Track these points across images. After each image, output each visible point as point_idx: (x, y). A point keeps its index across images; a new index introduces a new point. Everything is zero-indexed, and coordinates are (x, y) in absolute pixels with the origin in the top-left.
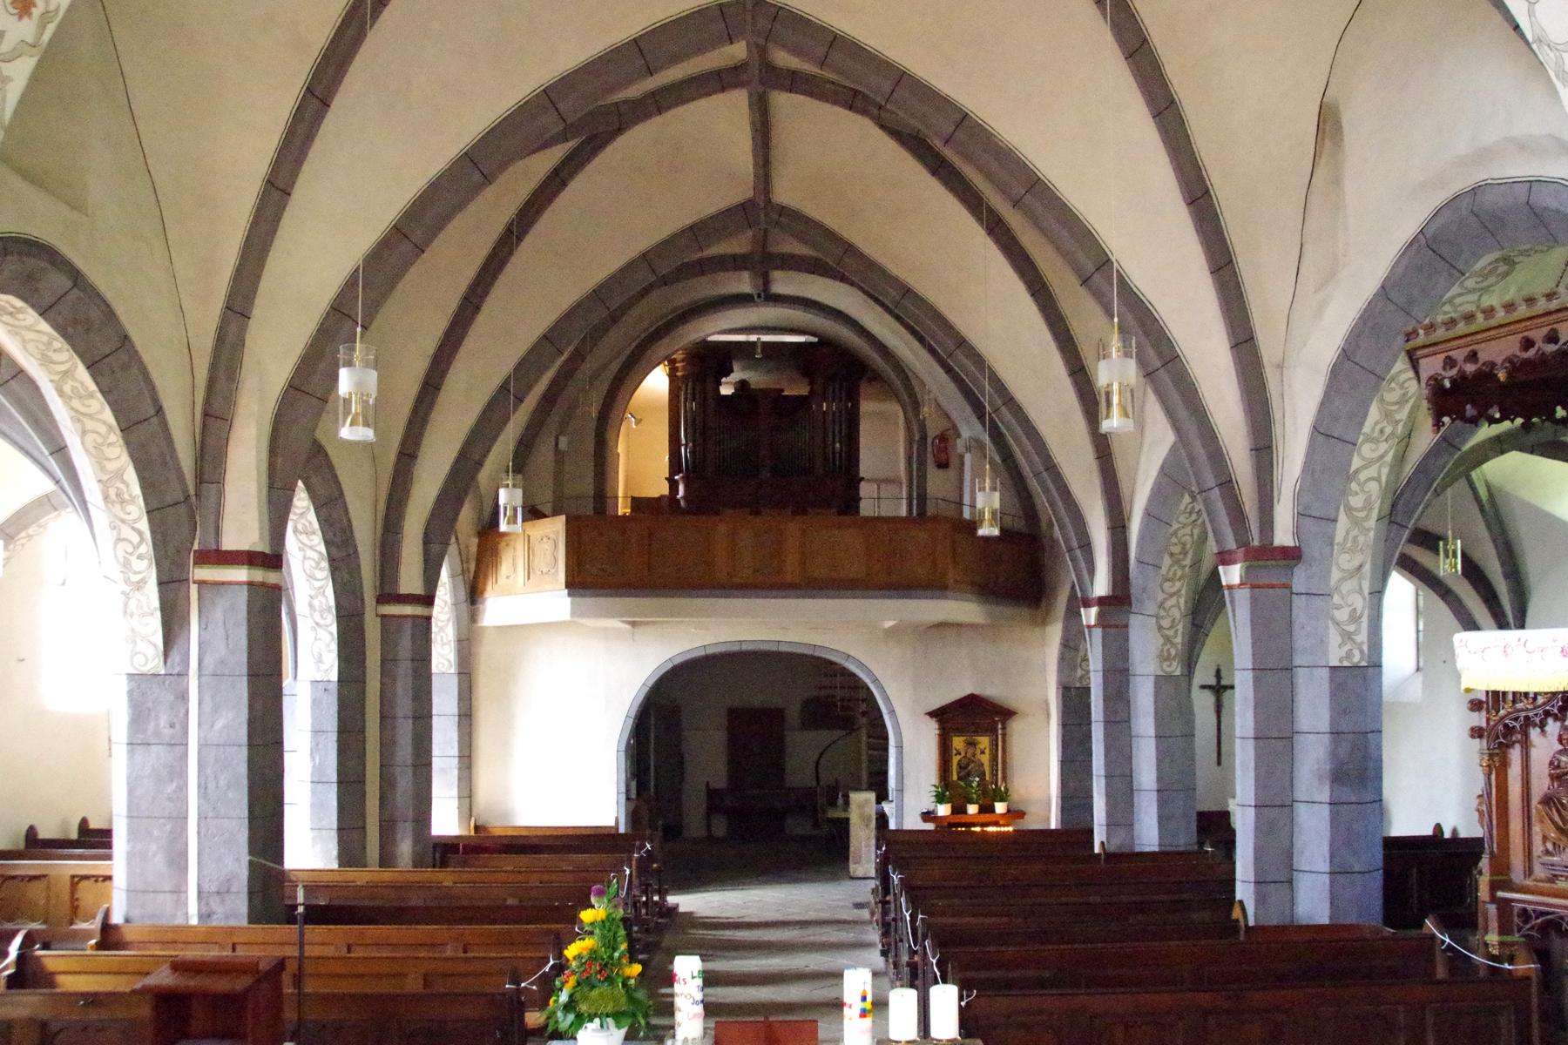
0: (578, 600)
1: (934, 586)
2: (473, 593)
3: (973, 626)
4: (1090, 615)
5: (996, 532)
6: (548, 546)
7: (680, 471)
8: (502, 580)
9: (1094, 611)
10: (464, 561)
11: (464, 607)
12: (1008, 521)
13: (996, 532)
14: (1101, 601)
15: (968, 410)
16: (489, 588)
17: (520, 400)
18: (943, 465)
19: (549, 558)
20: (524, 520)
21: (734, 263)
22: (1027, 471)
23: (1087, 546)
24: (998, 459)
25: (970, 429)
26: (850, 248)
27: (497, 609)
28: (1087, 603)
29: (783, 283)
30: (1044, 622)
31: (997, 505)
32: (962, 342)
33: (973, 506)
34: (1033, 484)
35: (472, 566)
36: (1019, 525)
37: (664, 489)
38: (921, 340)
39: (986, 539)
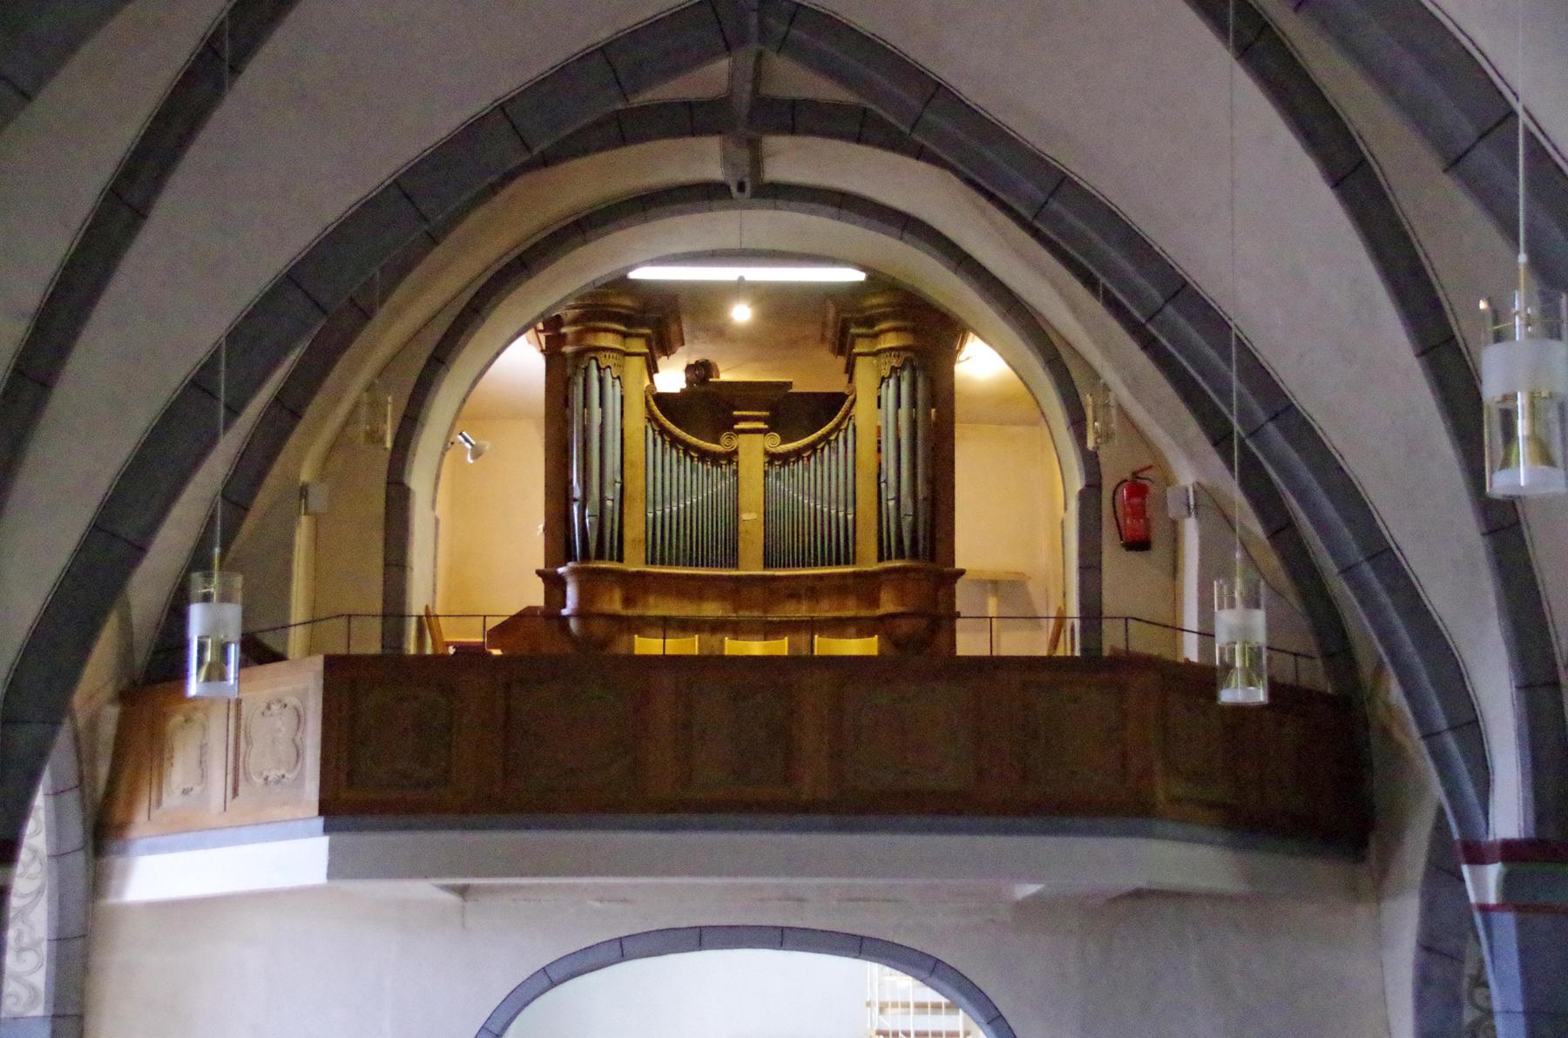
0: (347, 839)
1: (1122, 807)
2: (102, 833)
3: (1214, 897)
4: (1485, 883)
5: (1260, 695)
6: (282, 724)
7: (569, 556)
8: (172, 798)
9: (1493, 872)
10: (84, 755)
11: (79, 861)
12: (1287, 670)
13: (1260, 695)
14: (1510, 851)
15: (1193, 428)
16: (141, 817)
17: (234, 411)
18: (1138, 544)
19: (286, 750)
20: (243, 664)
21: (691, 119)
22: (1328, 565)
23: (1470, 727)
24: (1258, 529)
25: (1191, 467)
26: (937, 93)
27: (153, 874)
28: (1477, 854)
29: (791, 159)
30: (1378, 887)
31: (1260, 638)
32: (1180, 290)
33: (1207, 635)
34: (1339, 586)
35: (103, 770)
36: (1315, 676)
37: (536, 595)
38: (1089, 281)
39: (1238, 710)
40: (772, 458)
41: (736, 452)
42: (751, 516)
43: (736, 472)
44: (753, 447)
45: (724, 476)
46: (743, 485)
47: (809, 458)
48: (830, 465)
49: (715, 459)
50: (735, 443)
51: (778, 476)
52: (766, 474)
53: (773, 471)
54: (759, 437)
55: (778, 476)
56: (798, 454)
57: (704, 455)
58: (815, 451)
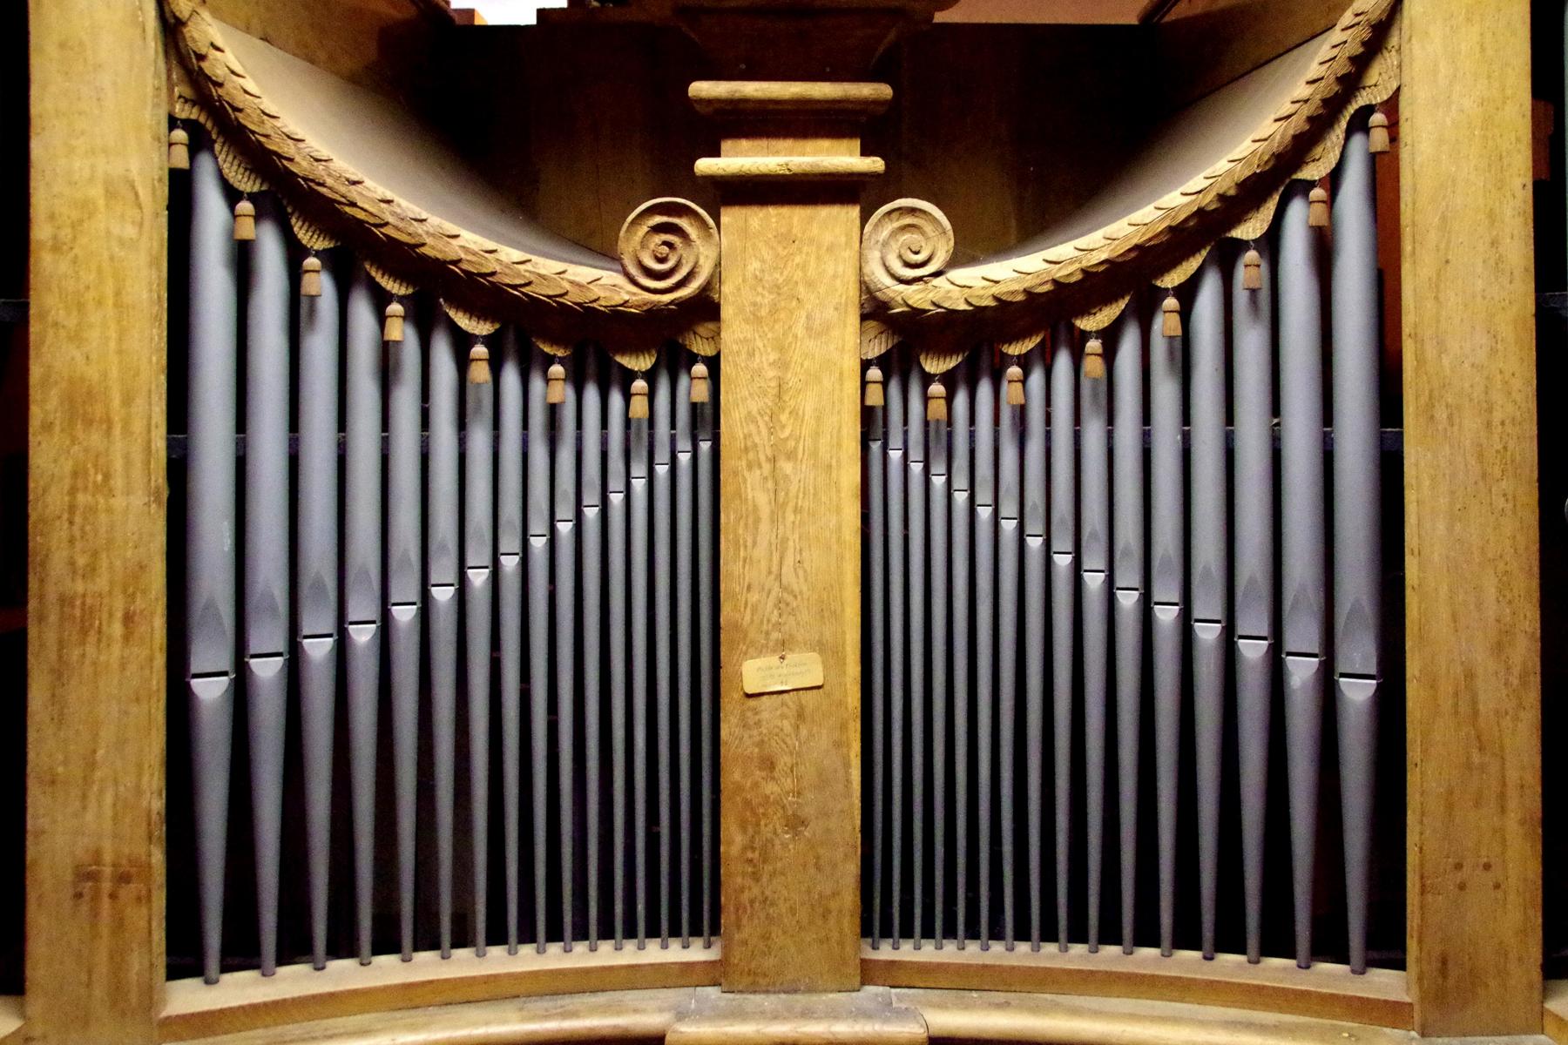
40: (907, 339)
41: (705, 308)
42: (792, 670)
43: (706, 419)
44: (800, 284)
45: (639, 437)
46: (747, 488)
47: (1110, 338)
48: (1242, 395)
49: (592, 343)
50: (699, 254)
51: (938, 439)
52: (871, 423)
53: (914, 410)
54: (835, 222)
55: (938, 439)
56: (1050, 315)
57: (529, 327)
58: (1144, 312)
